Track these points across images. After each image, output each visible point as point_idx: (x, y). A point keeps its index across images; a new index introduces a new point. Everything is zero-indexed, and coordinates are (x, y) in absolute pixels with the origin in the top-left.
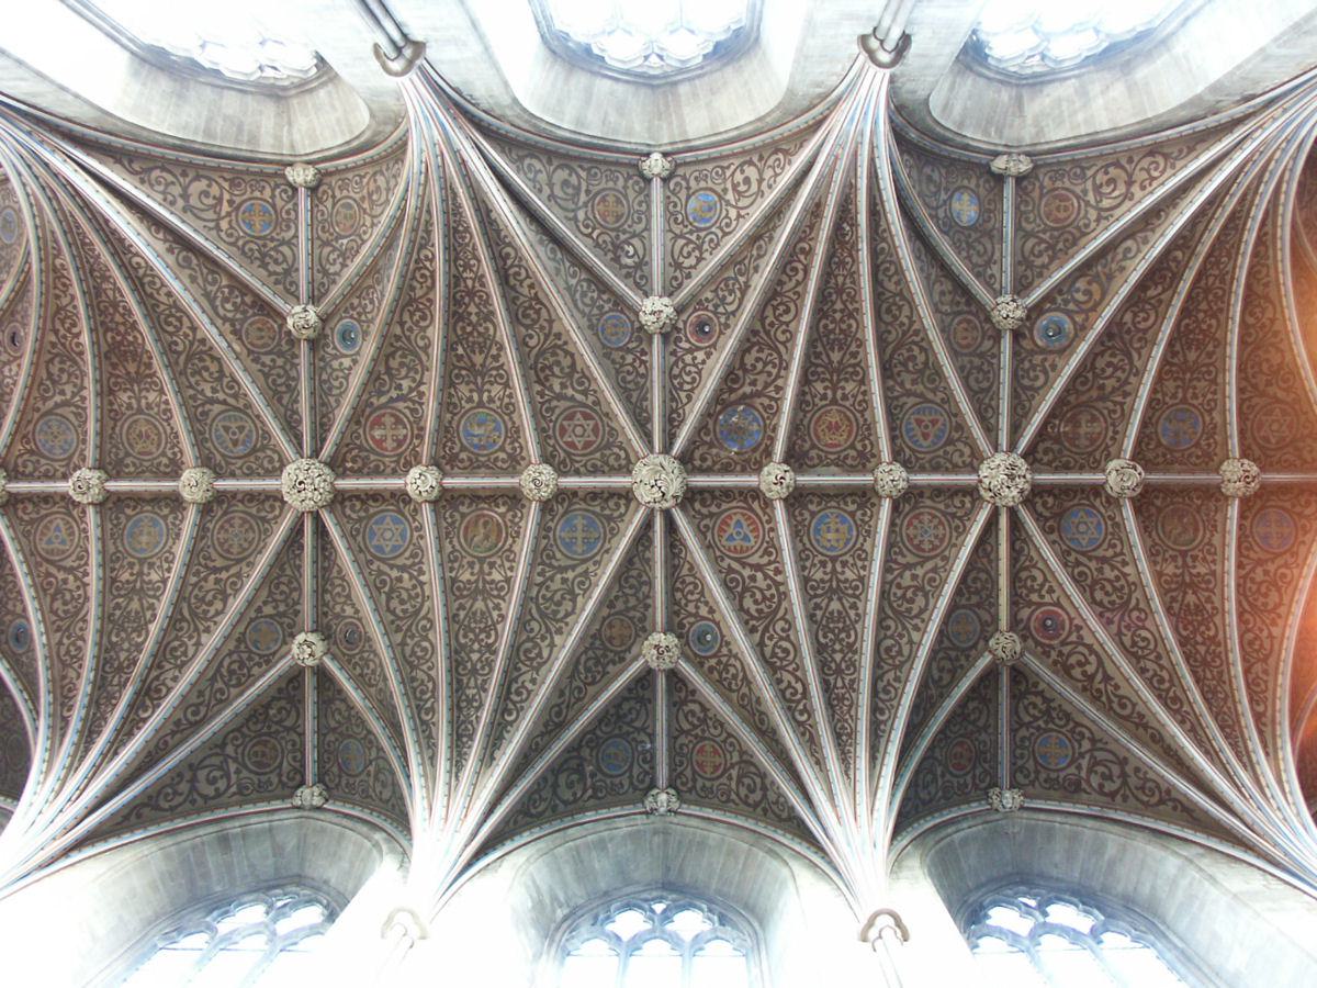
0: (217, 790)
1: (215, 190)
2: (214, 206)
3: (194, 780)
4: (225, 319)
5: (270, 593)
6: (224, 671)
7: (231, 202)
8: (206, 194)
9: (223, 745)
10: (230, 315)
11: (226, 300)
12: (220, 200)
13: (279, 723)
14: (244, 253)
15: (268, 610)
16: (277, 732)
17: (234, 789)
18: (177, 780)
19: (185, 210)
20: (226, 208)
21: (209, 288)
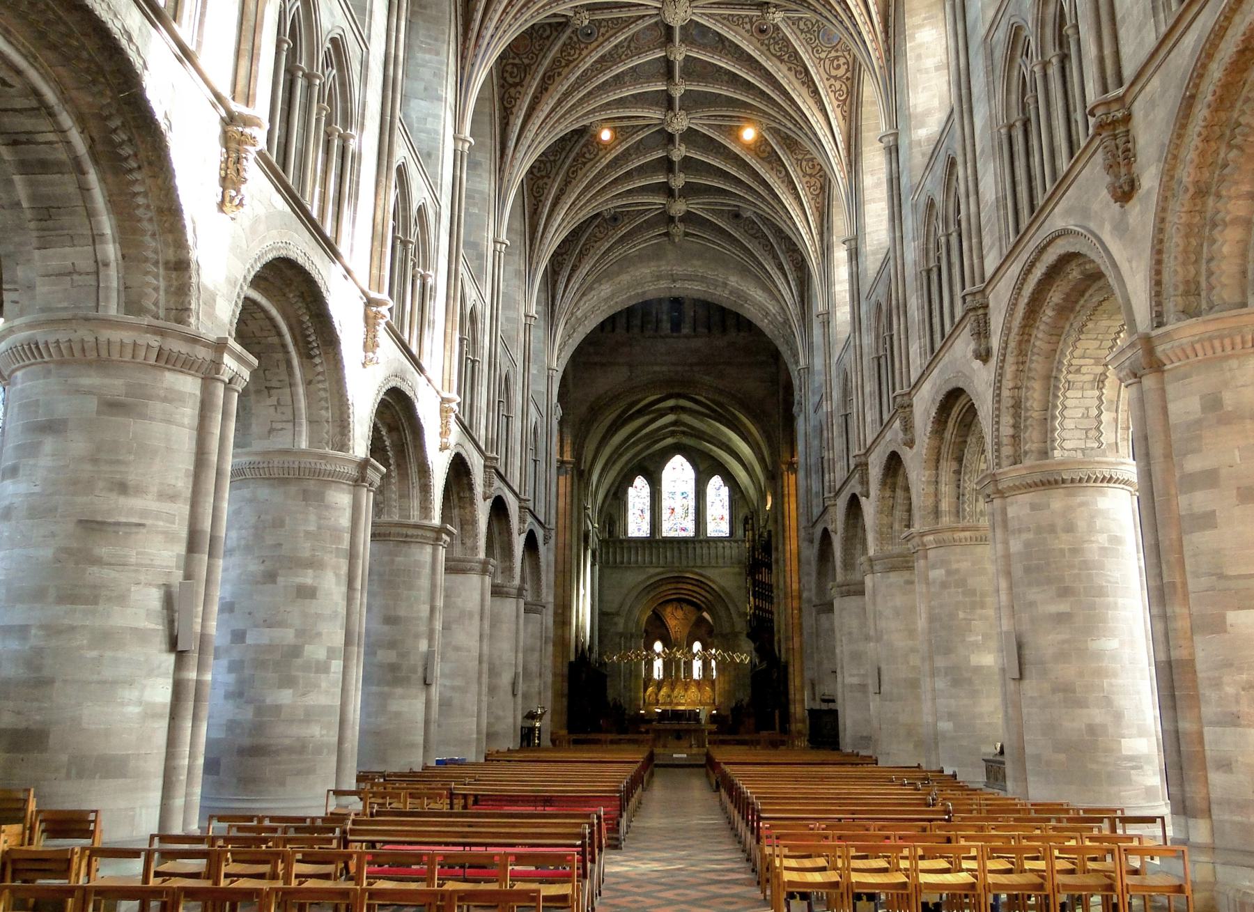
0: (844, 64)
1: (509, 68)
2: (518, 69)
3: (836, 78)
4: (580, 54)
5: (738, 25)
6: (779, 54)
7: (514, 58)
8: (511, 73)
9: (820, 59)
10: (577, 52)
11: (569, 54)
12: (514, 65)
13: (813, 26)
14: (542, 50)
15: (748, 27)
16: (819, 26)
17: (846, 53)
18: (833, 88)
19: (522, 86)
20: (517, 61)
21: (563, 64)
